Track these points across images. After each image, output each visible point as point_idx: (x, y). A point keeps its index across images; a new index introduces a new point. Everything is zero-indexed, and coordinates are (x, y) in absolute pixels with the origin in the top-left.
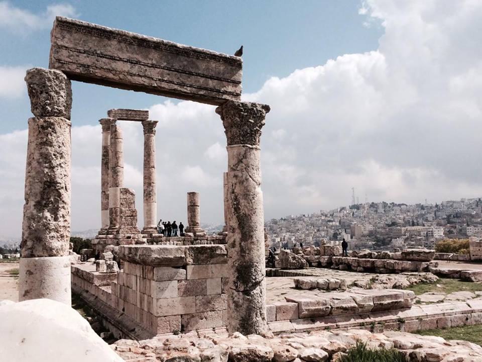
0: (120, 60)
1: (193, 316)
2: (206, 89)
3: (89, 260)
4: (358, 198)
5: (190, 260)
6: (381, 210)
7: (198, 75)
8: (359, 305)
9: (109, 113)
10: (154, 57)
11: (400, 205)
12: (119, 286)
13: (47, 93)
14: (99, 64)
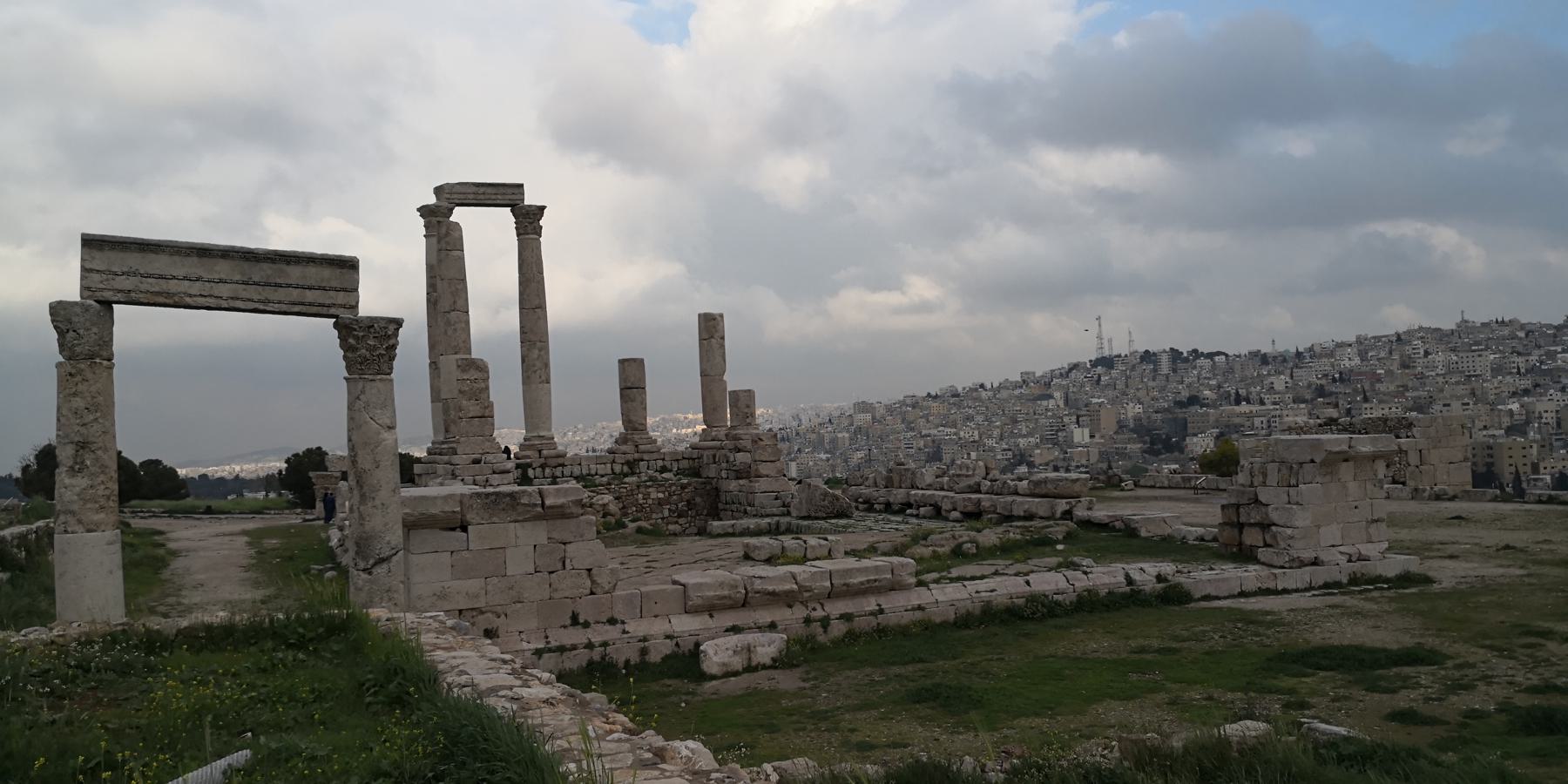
0: (174, 278)
1: (482, 613)
2: (303, 304)
4: (1110, 341)
6: (1165, 367)
7: (289, 286)
8: (800, 587)
9: (438, 191)
10: (223, 268)
11: (1211, 356)
14: (144, 287)
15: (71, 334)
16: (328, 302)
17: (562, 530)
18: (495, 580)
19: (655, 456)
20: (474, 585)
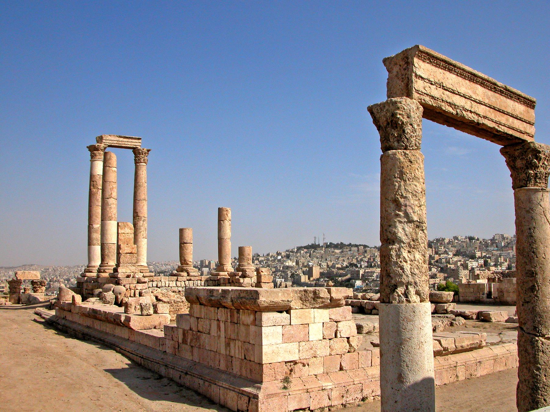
2: (513, 129)
3: (88, 300)
5: (292, 304)
11: (356, 246)
12: (180, 332)
13: (411, 125)
15: (410, 127)
16: (523, 129)
17: (336, 313)
18: (303, 343)
19: (197, 278)
20: (294, 346)
